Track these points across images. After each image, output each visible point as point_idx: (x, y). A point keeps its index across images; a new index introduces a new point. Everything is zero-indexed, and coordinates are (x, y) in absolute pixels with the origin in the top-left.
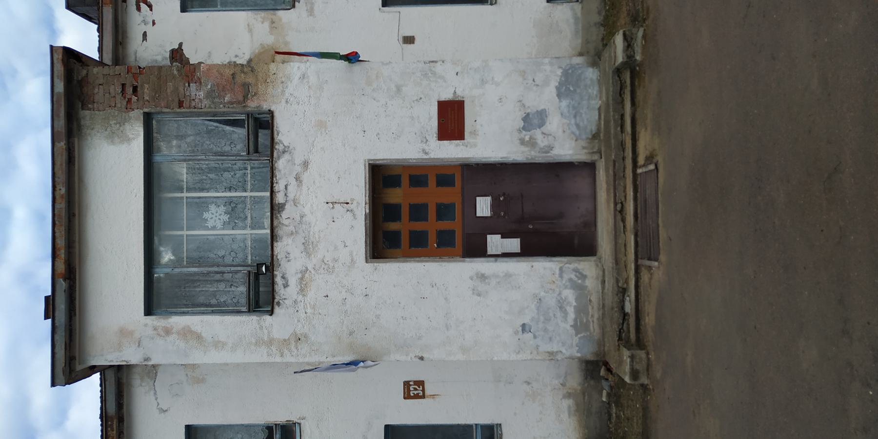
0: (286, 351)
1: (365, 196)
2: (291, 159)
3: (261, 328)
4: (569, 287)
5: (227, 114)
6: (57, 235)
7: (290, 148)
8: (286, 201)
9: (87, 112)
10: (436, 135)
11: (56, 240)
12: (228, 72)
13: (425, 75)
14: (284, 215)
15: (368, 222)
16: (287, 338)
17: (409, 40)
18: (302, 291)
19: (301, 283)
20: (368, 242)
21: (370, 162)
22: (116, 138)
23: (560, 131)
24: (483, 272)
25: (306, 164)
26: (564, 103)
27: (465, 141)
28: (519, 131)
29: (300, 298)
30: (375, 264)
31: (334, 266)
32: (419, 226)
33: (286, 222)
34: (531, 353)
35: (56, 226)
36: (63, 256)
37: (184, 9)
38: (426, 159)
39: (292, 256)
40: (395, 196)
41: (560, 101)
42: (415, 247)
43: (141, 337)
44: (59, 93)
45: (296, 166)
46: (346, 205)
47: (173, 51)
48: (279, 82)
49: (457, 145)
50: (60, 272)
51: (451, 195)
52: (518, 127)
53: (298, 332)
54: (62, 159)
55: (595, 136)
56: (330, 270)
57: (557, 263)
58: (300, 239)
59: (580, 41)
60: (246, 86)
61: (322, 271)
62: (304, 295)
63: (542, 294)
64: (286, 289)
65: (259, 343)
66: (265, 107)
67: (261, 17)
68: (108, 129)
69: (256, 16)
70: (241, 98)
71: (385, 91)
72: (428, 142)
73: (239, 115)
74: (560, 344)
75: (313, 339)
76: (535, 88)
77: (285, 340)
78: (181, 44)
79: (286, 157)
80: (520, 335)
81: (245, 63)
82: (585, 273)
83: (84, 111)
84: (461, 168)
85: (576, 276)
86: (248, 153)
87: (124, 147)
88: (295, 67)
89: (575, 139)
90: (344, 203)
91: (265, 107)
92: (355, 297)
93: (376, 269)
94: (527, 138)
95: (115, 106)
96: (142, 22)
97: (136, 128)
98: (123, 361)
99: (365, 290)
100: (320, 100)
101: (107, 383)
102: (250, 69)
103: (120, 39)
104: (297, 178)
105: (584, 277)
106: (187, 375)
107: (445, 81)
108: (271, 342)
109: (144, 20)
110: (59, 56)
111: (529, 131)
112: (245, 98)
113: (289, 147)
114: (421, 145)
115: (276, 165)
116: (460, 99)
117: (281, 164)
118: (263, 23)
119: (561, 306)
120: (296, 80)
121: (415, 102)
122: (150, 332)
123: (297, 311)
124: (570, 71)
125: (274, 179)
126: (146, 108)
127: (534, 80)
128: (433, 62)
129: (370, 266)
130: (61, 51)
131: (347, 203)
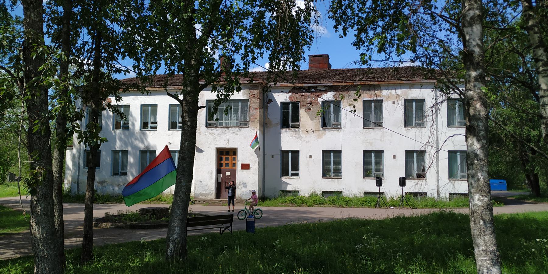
10: (242, 163)
17: (273, 157)
18: (210, 134)
25: (237, 134)
26: (248, 192)
47: (271, 100)
51: (230, 166)
55: (241, 198)
56: (214, 140)
60: (254, 121)
66: (249, 126)
79: (239, 130)
104: (234, 132)
105: (211, 195)
112: (251, 121)
117: (237, 129)
119: (205, 190)
122: (203, 101)
129: (215, 148)
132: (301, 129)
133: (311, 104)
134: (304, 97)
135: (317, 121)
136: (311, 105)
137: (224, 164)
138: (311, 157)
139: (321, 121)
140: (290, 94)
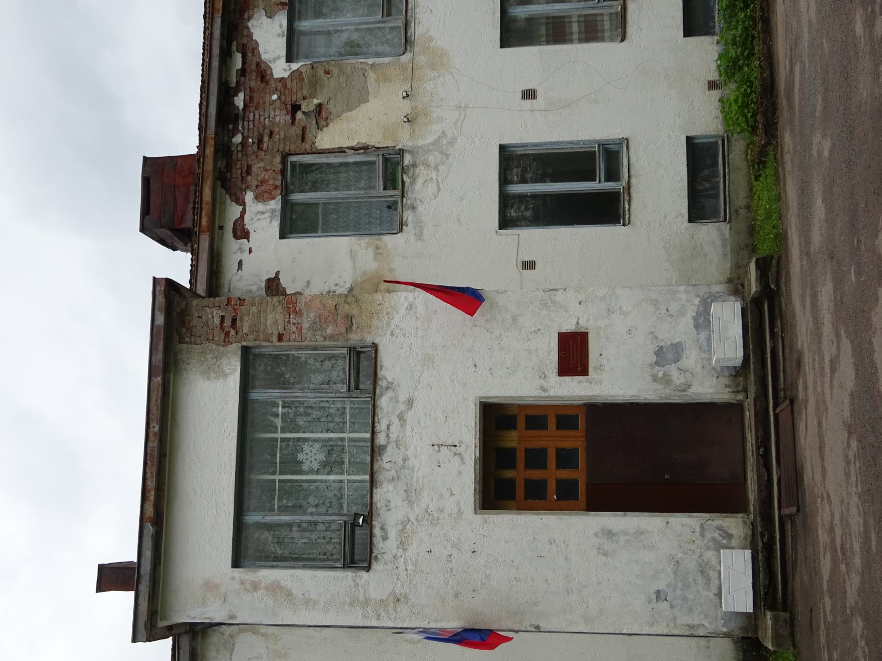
0: (383, 614)
1: (475, 438)
2: (394, 396)
3: (356, 586)
4: (712, 547)
5: (328, 347)
6: (148, 475)
7: (394, 384)
8: (388, 443)
9: (184, 346)
10: (556, 370)
11: (147, 481)
12: (331, 303)
13: (544, 304)
14: (386, 457)
15: (478, 467)
16: (384, 598)
17: (529, 265)
19: (401, 536)
20: (478, 490)
21: (482, 400)
22: (212, 373)
23: (699, 366)
24: (610, 528)
25: (410, 402)
27: (589, 377)
28: (652, 366)
29: (400, 552)
30: (486, 516)
31: (438, 517)
32: (537, 474)
33: (388, 466)
34: (668, 626)
35: (148, 466)
36: (152, 498)
37: (282, 236)
38: (544, 397)
39: (392, 505)
40: (512, 439)
41: (698, 334)
42: (531, 499)
43: (227, 591)
44: (159, 325)
45: (400, 404)
46: (453, 447)
48: (385, 312)
49: (580, 382)
50: (148, 516)
52: (650, 362)
53: (397, 592)
54: (157, 395)
56: (434, 522)
57: (697, 519)
58: (401, 486)
59: (729, 265)
60: (350, 318)
61: (425, 522)
62: (404, 550)
63: (680, 555)
64: (385, 542)
65: (353, 603)
66: (369, 339)
67: (365, 243)
68: (205, 364)
69: (359, 242)
70: (343, 330)
71: (500, 322)
72: (547, 378)
73: (340, 349)
74: (702, 616)
75: (414, 600)
76: (669, 319)
77: (382, 601)
78: (278, 273)
79: (390, 393)
80: (654, 605)
81: (346, 293)
82: (730, 532)
83: (182, 345)
84: (584, 407)
85: (721, 536)
86: (349, 390)
87: (220, 383)
88: (404, 297)
89: (716, 375)
90: (452, 446)
91: (368, 339)
92: (462, 553)
93: (486, 522)
94: (660, 374)
95: (213, 339)
96: (238, 249)
97: (233, 363)
98: (206, 618)
99: (473, 545)
100: (428, 331)
101: (181, 652)
102: (354, 299)
103: (215, 269)
104: (401, 418)
106: (268, 648)
107: (567, 311)
108: (367, 602)
109: (240, 248)
110: (161, 288)
111: (663, 366)
112: (349, 329)
113: (392, 383)
114: (539, 381)
115: (378, 402)
116: (583, 330)
117: (384, 402)
118: (366, 249)
120: (403, 311)
121: (533, 334)
122: (236, 585)
123: (397, 568)
124: (709, 300)
125: (376, 418)
126: (244, 341)
127: (667, 310)
128: (552, 290)
129: (479, 519)
130: (163, 282)
131: (455, 446)
132: (404, 140)
133: (296, 108)
134: (266, 139)
135: (371, 75)
136: (304, 108)
137: (565, 474)
138: (529, 94)
139: (370, 61)
140: (249, 196)
